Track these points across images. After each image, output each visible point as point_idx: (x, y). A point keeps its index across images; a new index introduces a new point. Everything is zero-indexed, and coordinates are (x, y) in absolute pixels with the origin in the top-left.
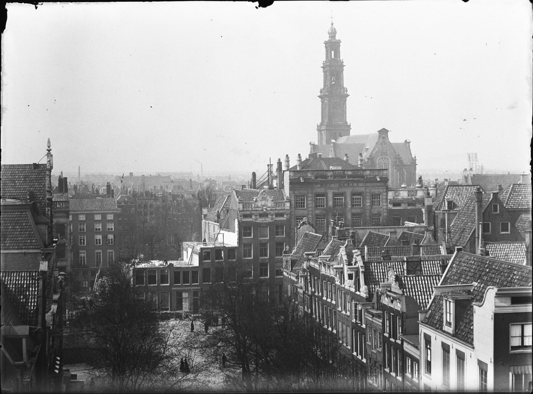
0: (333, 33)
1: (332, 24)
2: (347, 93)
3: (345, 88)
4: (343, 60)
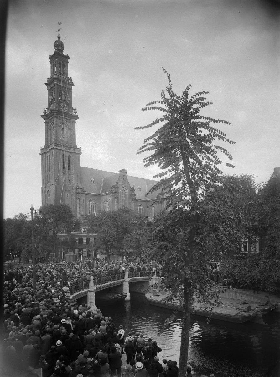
1: (59, 38)
2: (76, 114)
3: (73, 109)
4: (71, 78)
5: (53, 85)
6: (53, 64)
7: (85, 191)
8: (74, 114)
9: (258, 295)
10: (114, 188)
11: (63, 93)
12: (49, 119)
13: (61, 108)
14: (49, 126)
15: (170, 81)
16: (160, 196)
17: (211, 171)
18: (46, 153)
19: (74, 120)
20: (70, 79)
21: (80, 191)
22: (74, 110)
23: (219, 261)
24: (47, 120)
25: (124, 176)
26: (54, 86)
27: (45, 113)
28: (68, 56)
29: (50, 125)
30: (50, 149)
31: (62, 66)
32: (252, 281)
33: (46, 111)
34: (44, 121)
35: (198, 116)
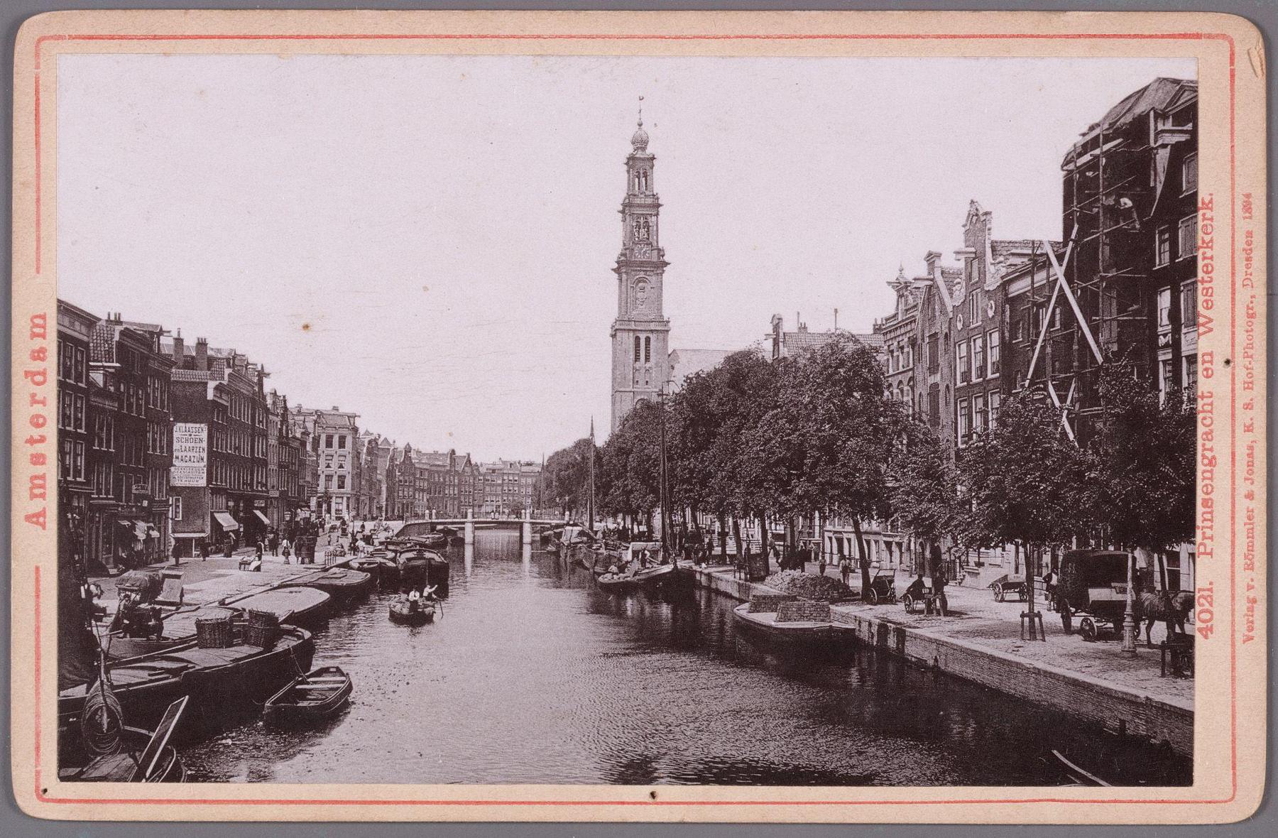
0: (641, 143)
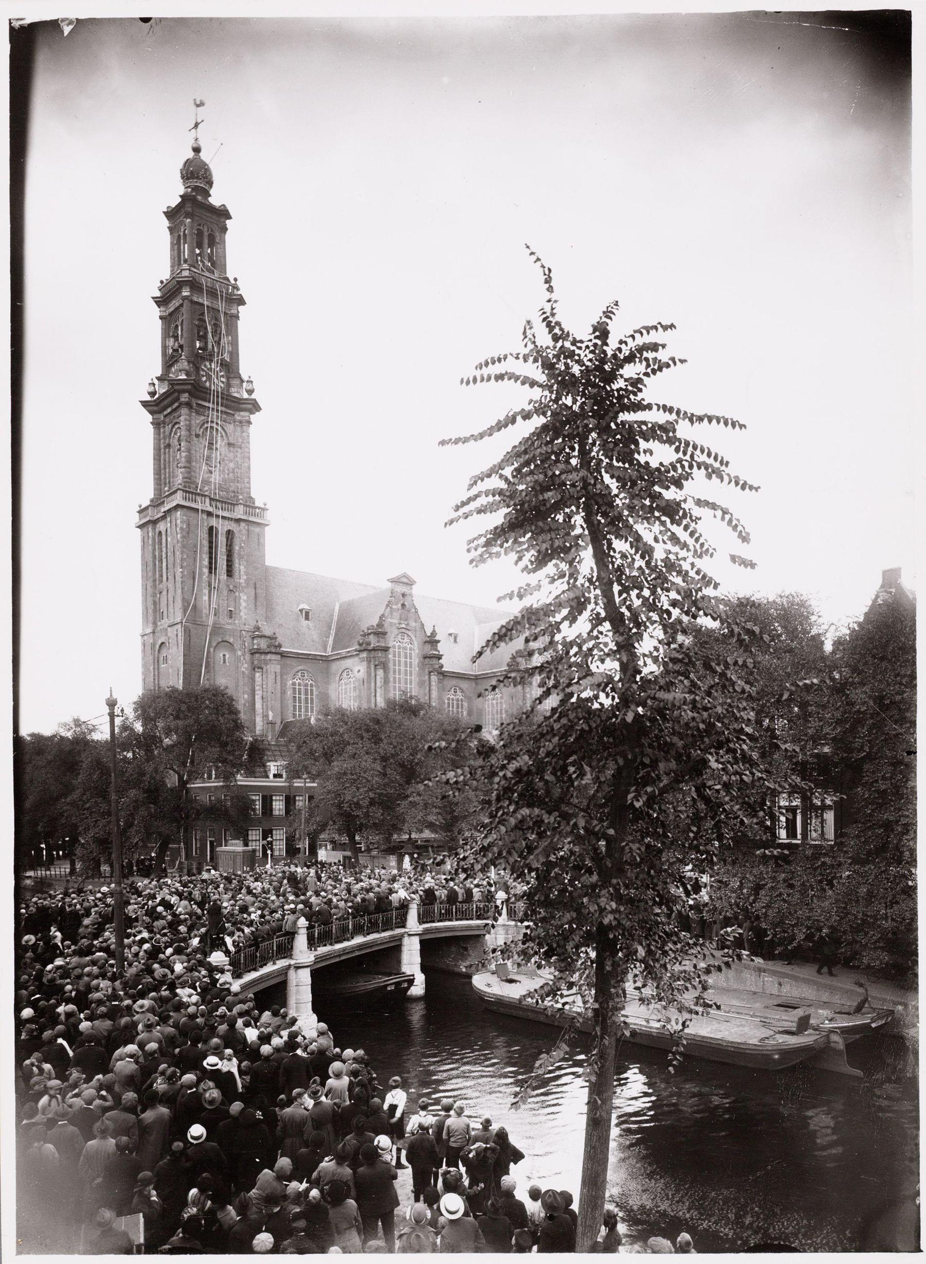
1: (197, 150)
2: (253, 396)
3: (242, 381)
4: (236, 280)
5: (177, 304)
6: (176, 235)
7: (280, 646)
8: (246, 396)
9: (832, 978)
10: (372, 637)
11: (209, 328)
12: (165, 413)
13: (203, 376)
14: (164, 432)
15: (550, 289)
16: (519, 660)
17: (684, 581)
18: (154, 522)
19: (247, 414)
20: (233, 282)
21: (263, 644)
22: (245, 384)
23: (707, 869)
24: (156, 416)
25: (404, 595)
26: (182, 305)
27: (152, 394)
28: (227, 211)
29: (167, 433)
30: (166, 509)
31: (206, 241)
32: (813, 935)
33: (157, 387)
34: (149, 418)
35: (639, 402)
